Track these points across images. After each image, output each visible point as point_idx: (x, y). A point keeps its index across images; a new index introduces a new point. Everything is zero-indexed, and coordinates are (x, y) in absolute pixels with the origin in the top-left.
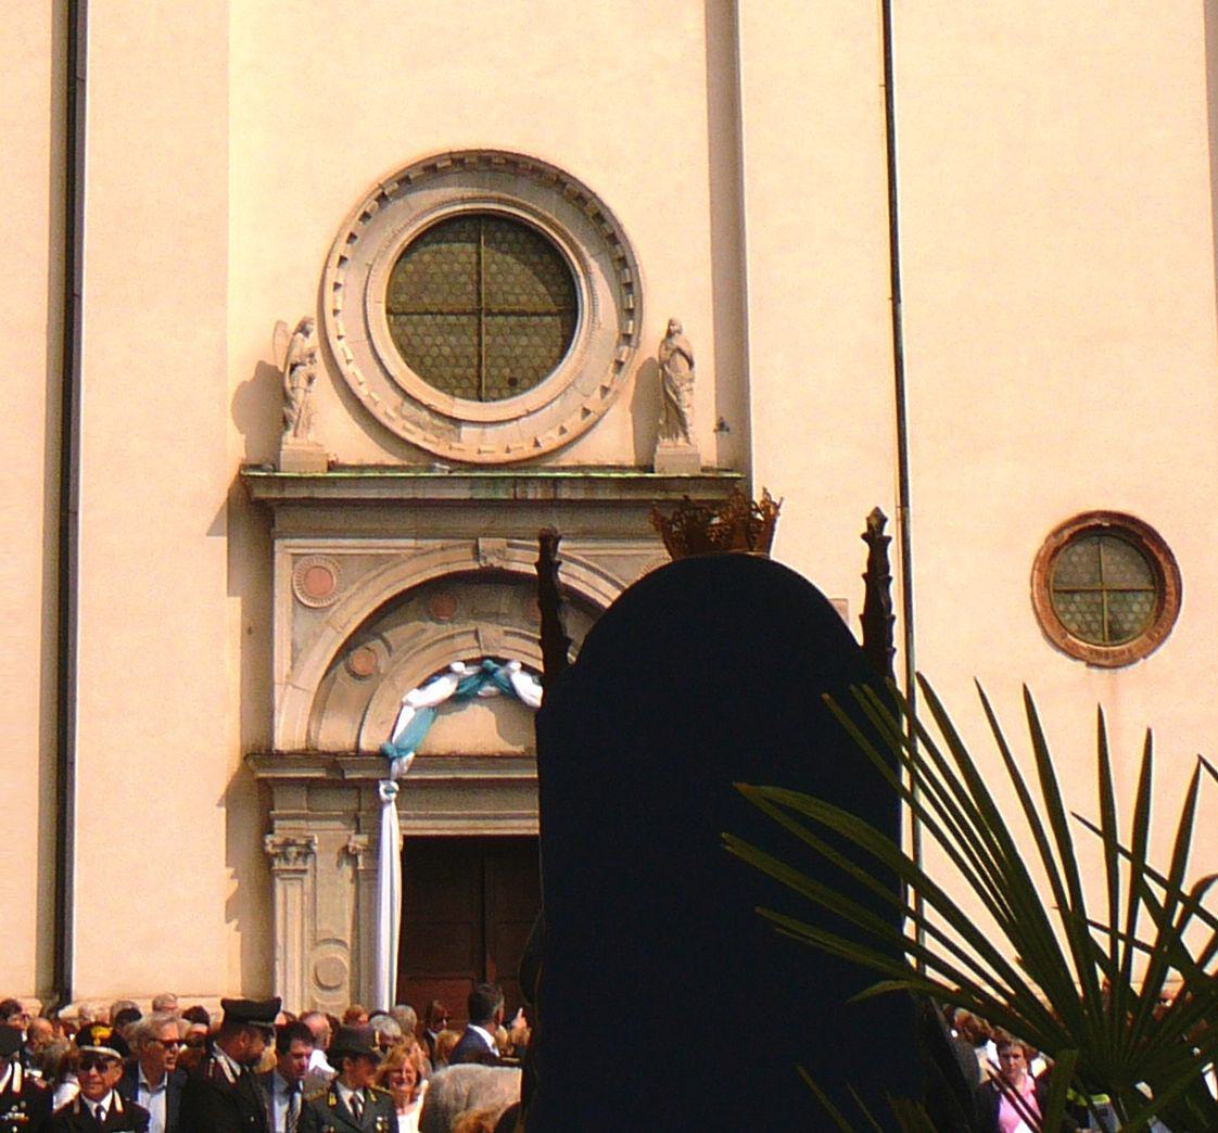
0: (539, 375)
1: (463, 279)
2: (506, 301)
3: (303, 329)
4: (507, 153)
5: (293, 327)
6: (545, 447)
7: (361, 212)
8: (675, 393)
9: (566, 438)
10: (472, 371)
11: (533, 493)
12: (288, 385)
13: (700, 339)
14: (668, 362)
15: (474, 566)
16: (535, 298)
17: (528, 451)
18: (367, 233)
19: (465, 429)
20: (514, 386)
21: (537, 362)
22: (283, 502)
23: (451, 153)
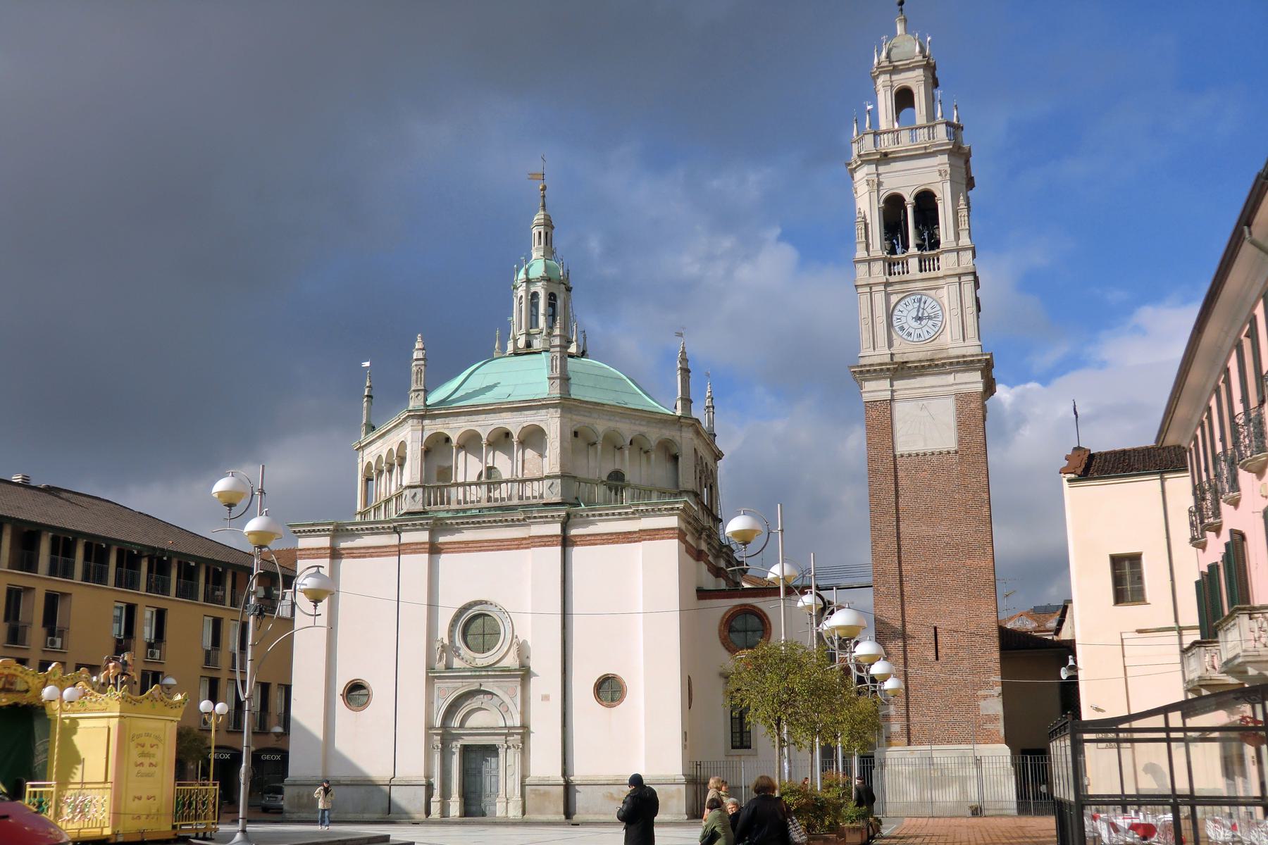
11: (484, 673)
20: (489, 650)
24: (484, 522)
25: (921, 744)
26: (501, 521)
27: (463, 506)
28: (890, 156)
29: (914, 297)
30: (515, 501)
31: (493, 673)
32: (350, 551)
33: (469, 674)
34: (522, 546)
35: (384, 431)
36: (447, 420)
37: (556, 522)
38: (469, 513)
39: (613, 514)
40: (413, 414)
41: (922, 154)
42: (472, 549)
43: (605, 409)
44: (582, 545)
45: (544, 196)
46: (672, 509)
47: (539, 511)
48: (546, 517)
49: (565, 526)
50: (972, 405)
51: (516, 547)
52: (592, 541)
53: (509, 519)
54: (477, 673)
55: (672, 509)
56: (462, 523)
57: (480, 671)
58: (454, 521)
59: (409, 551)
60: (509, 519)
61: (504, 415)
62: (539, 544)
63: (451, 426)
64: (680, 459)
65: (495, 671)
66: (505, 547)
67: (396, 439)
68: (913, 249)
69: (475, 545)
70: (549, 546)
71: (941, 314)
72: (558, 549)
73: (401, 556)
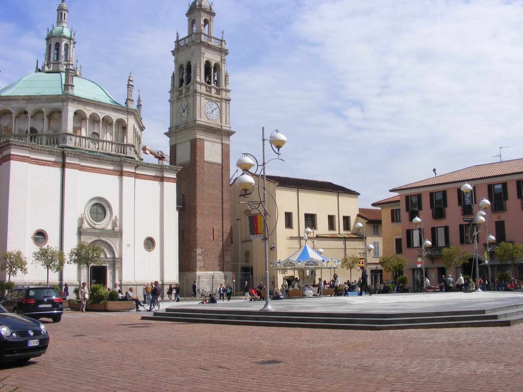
0: (102, 220)
13: (118, 217)
15: (99, 239)
17: (102, 228)
20: (100, 221)
24: (103, 159)
25: (208, 271)
28: (210, 46)
29: (211, 102)
34: (117, 174)
35: (33, 98)
41: (218, 50)
42: (97, 172)
44: (140, 179)
46: (176, 170)
47: (129, 161)
48: (132, 163)
49: (136, 168)
50: (227, 149)
51: (115, 174)
53: (114, 161)
55: (176, 170)
56: (94, 158)
62: (126, 175)
67: (46, 105)
68: (213, 85)
69: (98, 170)
70: (129, 176)
71: (219, 112)
73: (67, 170)
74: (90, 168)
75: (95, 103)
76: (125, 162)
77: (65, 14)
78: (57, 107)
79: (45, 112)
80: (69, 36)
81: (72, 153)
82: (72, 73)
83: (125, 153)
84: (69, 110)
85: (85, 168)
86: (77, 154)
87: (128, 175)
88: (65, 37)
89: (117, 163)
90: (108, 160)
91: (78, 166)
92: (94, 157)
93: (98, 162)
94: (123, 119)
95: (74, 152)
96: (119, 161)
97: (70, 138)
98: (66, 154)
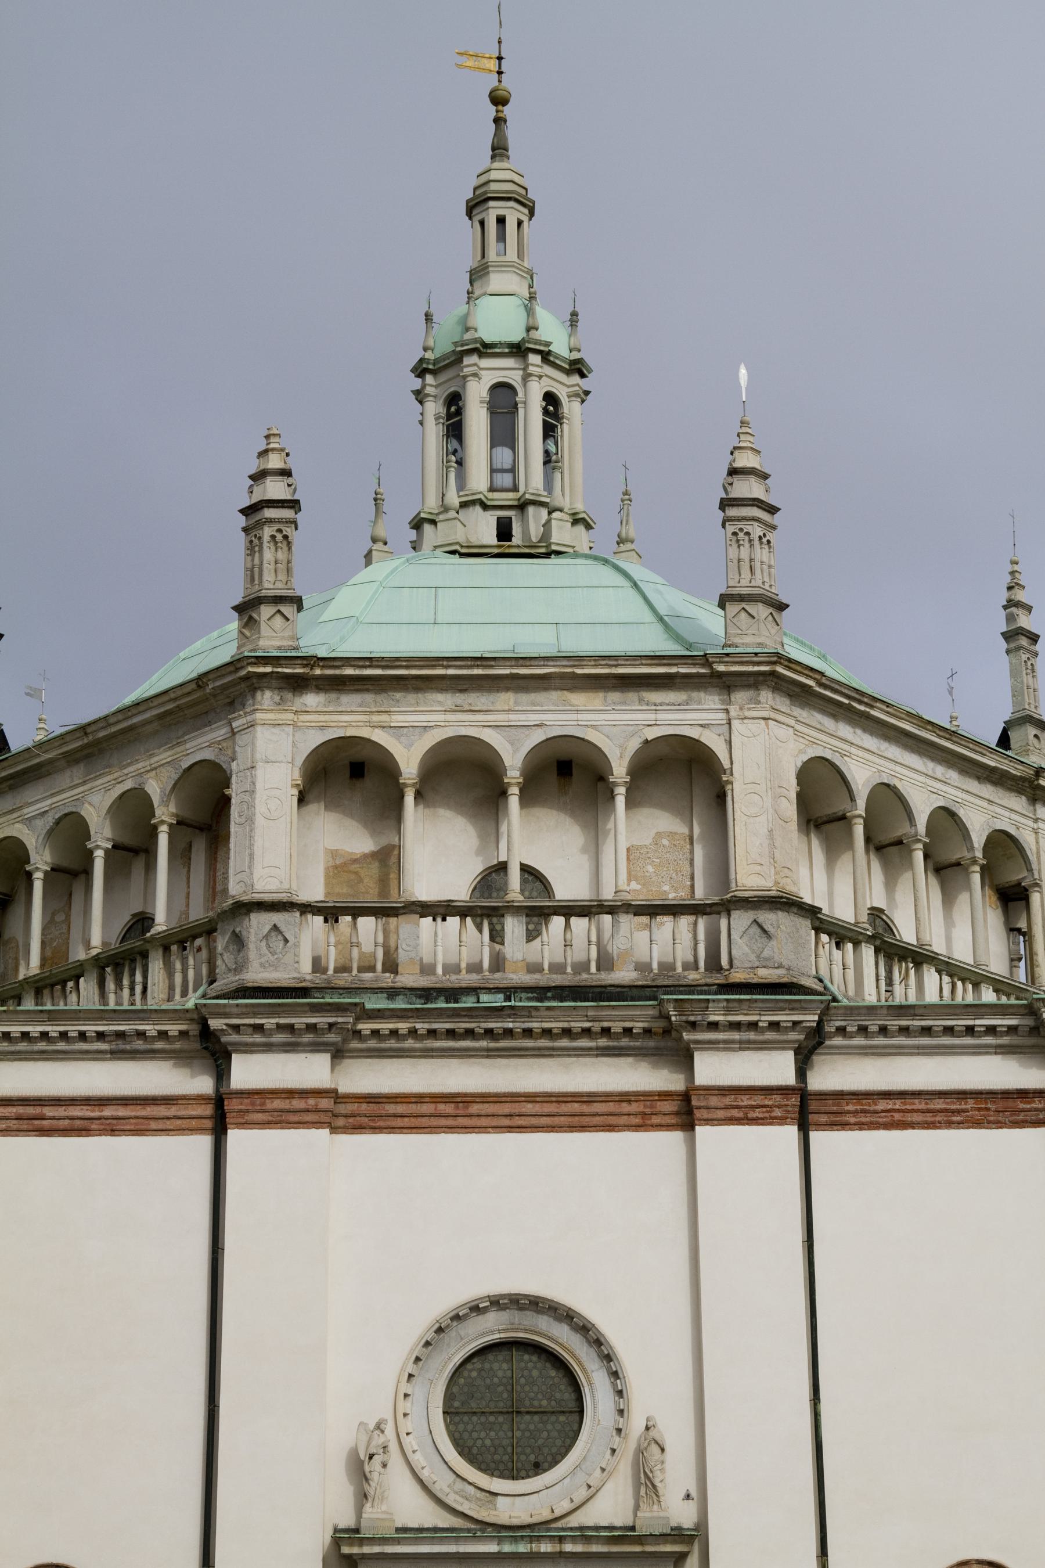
1: (500, 1389)
2: (532, 1406)
3: (379, 1427)
4: (529, 1296)
5: (372, 1426)
6: (558, 1513)
7: (423, 1341)
8: (651, 1472)
9: (573, 1506)
10: (506, 1458)
11: (545, 1547)
12: (367, 1468)
14: (646, 1449)
16: (553, 1403)
17: (546, 1515)
18: (428, 1356)
19: (500, 1498)
20: (538, 1468)
21: (554, 1450)
22: (364, 1557)
23: (489, 1296)
24: (528, 1033)
26: (587, 1032)
27: (439, 978)
30: (624, 975)
31: (579, 1548)
32: (31, 1111)
33: (492, 1548)
34: (656, 1120)
35: (101, 734)
36: (382, 701)
37: (784, 1049)
38: (468, 1002)
39: (970, 1030)
40: (268, 669)
42: (484, 1122)
43: (875, 713)
44: (861, 1126)
45: (499, 121)
47: (728, 1011)
48: (753, 1026)
52: (897, 1116)
53: (617, 1027)
54: (522, 1548)
56: (451, 1034)
57: (531, 1539)
58: (422, 1026)
59: (260, 1117)
60: (617, 1027)
61: (578, 698)
62: (721, 1114)
63: (398, 719)
64: (1035, 898)
65: (588, 1540)
66: (597, 1120)
67: (164, 756)
72: (791, 1132)
73: (235, 1137)
74: (426, 1108)
75: (451, 672)
76: (693, 1025)
77: (501, 221)
78: (208, 755)
79: (165, 803)
80: (516, 335)
81: (259, 1028)
82: (279, 521)
83: (724, 962)
84: (258, 756)
85: (391, 1109)
86: (300, 1021)
87: (735, 1113)
88: (485, 349)
89: (651, 1043)
90: (567, 1032)
91: (325, 1103)
92: (448, 1026)
93: (489, 1054)
94: (694, 733)
95: (278, 1014)
96: (658, 1025)
97: (275, 928)
98: (224, 1039)
